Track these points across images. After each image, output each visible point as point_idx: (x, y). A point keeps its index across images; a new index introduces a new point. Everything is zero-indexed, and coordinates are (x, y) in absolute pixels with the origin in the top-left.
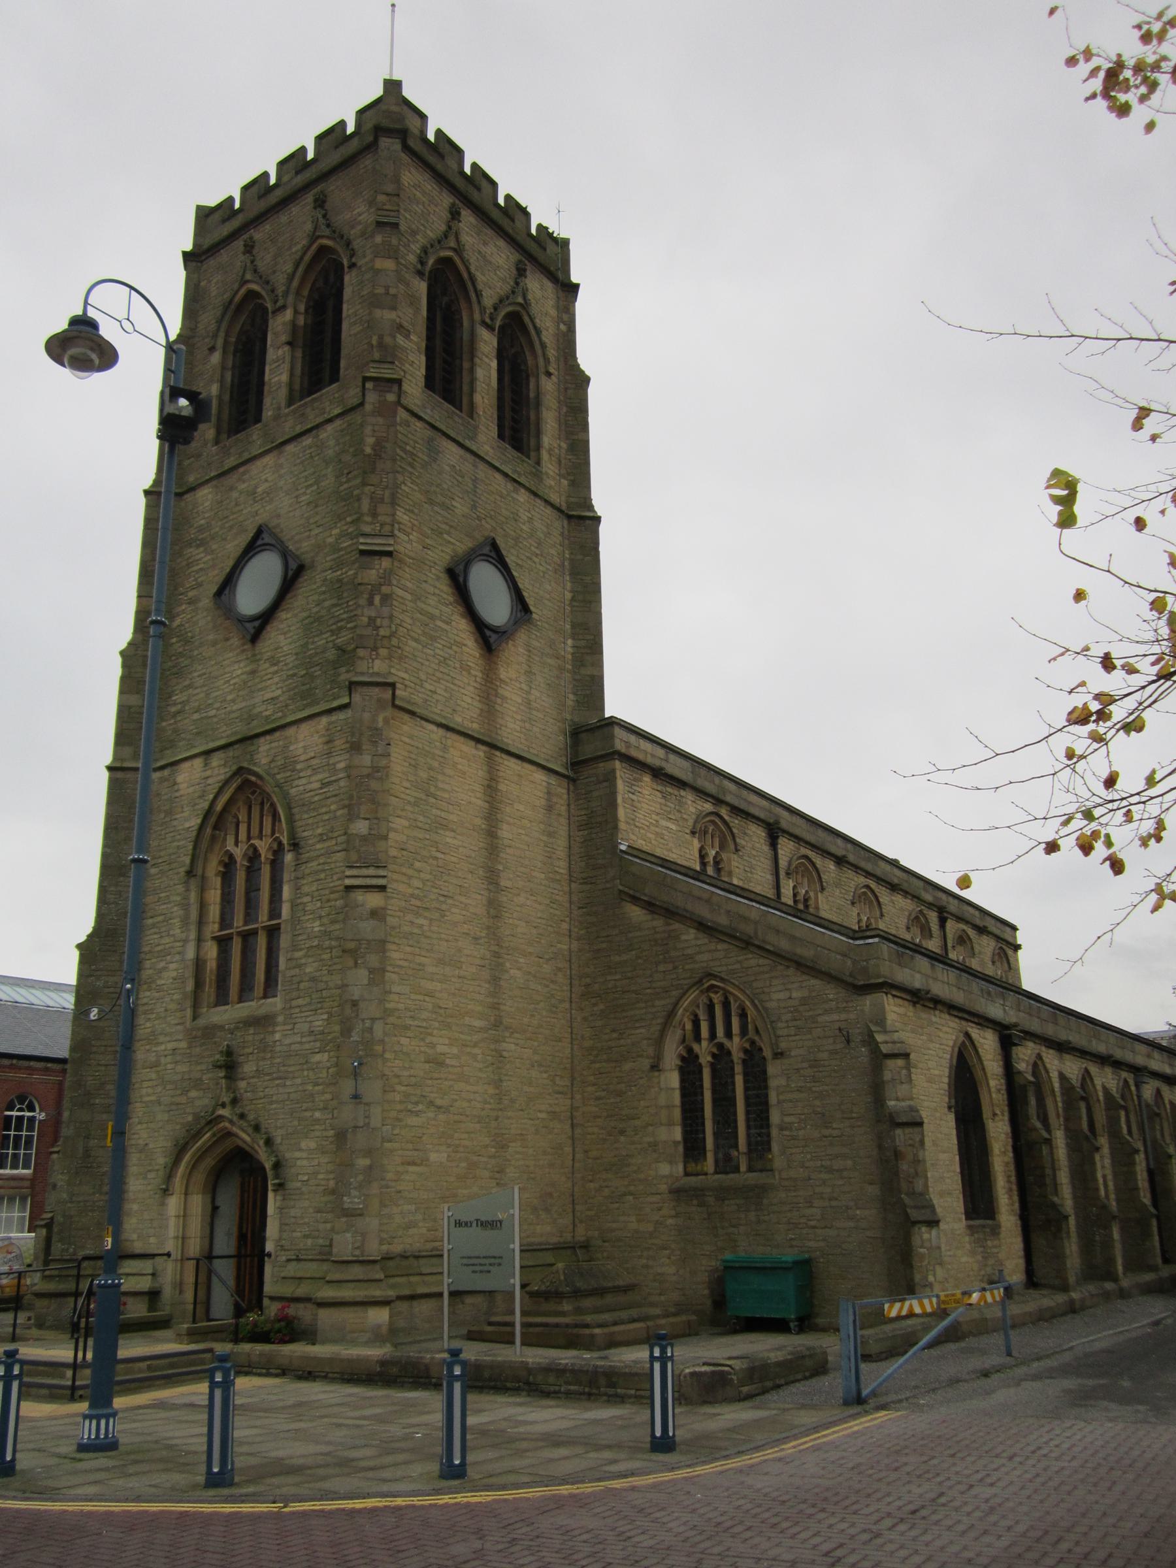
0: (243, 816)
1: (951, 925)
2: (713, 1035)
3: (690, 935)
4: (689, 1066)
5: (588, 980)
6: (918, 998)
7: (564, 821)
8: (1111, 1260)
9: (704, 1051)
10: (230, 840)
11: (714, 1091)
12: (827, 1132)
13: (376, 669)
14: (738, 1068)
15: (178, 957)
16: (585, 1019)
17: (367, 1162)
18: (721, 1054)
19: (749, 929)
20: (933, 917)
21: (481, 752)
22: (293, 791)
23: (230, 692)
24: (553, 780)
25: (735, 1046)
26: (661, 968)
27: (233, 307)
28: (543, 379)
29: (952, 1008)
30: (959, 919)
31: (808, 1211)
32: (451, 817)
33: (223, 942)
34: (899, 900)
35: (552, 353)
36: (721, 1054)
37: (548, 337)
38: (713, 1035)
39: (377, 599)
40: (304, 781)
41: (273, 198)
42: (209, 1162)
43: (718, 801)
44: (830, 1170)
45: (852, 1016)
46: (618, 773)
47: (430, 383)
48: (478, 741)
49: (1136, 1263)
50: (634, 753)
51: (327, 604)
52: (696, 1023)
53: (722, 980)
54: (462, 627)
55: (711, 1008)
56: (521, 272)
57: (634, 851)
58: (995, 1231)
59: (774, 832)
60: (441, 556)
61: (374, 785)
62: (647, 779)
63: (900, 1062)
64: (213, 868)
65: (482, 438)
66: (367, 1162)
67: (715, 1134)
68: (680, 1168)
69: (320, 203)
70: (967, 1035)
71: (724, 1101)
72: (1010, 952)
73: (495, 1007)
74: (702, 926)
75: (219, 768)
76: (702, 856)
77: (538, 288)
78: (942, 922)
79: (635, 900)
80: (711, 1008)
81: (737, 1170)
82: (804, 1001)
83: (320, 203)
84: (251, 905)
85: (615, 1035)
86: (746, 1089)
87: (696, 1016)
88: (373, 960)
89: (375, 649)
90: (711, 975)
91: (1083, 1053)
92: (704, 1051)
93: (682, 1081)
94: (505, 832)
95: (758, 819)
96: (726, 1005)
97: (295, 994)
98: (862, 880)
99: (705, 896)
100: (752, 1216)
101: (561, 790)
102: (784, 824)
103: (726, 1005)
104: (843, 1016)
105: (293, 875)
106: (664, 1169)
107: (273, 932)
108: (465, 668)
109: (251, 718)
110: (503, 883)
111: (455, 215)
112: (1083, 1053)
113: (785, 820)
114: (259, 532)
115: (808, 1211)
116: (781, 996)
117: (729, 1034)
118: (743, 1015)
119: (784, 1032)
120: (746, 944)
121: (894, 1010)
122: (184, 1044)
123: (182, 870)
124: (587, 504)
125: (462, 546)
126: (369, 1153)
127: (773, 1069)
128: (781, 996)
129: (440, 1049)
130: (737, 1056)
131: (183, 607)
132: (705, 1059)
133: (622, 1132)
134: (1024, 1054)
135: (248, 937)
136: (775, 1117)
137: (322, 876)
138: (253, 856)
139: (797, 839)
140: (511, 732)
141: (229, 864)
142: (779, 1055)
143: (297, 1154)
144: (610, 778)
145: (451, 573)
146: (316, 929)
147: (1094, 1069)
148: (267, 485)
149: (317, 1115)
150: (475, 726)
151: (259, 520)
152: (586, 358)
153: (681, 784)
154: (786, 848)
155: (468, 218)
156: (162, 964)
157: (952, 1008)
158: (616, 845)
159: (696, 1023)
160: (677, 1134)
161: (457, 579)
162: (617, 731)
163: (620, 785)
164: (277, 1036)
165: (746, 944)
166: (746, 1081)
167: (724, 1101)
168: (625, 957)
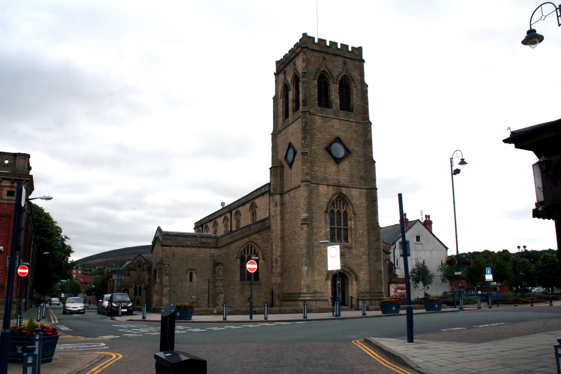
15: (324, 230)
23: (332, 173)
75: (331, 191)
105: (354, 220)
109: (339, 182)
123: (324, 210)
131: (315, 145)
137: (361, 222)
138: (339, 212)
143: (360, 274)
146: (361, 232)
149: (364, 267)
156: (320, 230)
164: (353, 251)
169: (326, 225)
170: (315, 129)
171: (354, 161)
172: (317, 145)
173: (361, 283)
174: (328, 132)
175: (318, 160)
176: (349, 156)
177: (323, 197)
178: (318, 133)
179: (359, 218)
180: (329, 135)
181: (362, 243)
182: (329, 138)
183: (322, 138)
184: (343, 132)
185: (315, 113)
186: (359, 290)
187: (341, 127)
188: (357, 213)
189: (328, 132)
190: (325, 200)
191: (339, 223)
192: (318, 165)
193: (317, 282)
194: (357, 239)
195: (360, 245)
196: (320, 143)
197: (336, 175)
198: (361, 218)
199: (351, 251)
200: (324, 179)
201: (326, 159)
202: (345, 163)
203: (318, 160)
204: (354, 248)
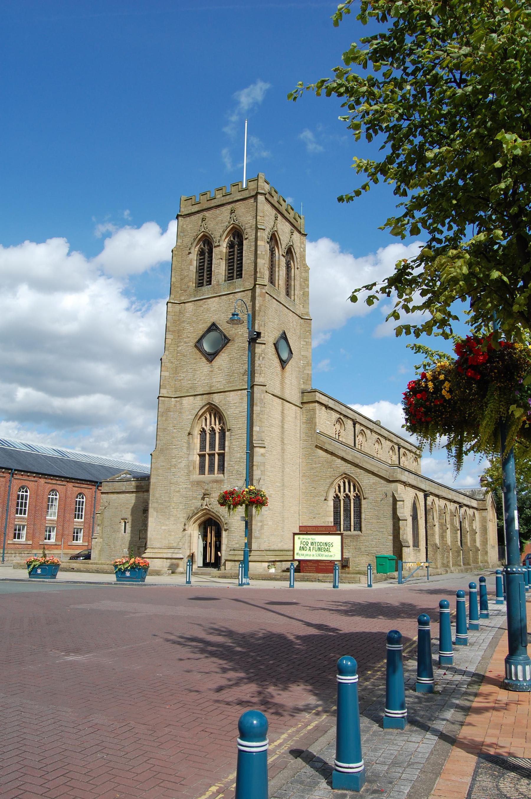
1: (402, 450)
2: (345, 491)
5: (304, 472)
6: (405, 484)
7: (299, 421)
8: (448, 562)
9: (342, 496)
11: (344, 508)
12: (378, 521)
13: (261, 381)
15: (186, 459)
16: (303, 483)
17: (261, 524)
18: (347, 496)
20: (396, 447)
21: (279, 401)
22: (228, 413)
23: (203, 377)
25: (352, 495)
26: (329, 470)
27: (198, 239)
29: (413, 487)
30: (404, 448)
31: (371, 543)
32: (274, 423)
33: (202, 456)
34: (388, 442)
38: (345, 491)
39: (261, 358)
40: (232, 410)
42: (199, 522)
44: (379, 532)
45: (388, 489)
46: (317, 407)
48: (280, 398)
49: (456, 564)
50: (321, 401)
51: (239, 354)
53: (349, 475)
54: (276, 362)
55: (344, 483)
56: (292, 233)
57: (321, 433)
59: (355, 423)
61: (261, 416)
62: (324, 408)
63: (401, 503)
64: (196, 432)
65: (281, 296)
66: (261, 524)
67: (344, 520)
69: (232, 212)
70: (416, 494)
71: (347, 511)
73: (283, 480)
74: (343, 459)
75: (199, 402)
78: (399, 449)
79: (321, 448)
80: (344, 483)
81: (350, 530)
82: (374, 483)
84: (212, 447)
85: (313, 489)
86: (354, 507)
87: (339, 485)
88: (262, 468)
89: (260, 374)
90: (345, 474)
91: (445, 498)
92: (342, 496)
93: (334, 504)
94: (286, 426)
95: (350, 418)
97: (231, 475)
99: (344, 449)
100: (355, 543)
104: (386, 489)
107: (222, 456)
110: (285, 442)
111: (276, 218)
112: (445, 498)
114: (214, 324)
115: (371, 543)
116: (367, 481)
117: (350, 491)
118: (354, 486)
119: (367, 492)
120: (357, 466)
121: (400, 487)
122: (190, 486)
126: (261, 521)
127: (363, 502)
128: (367, 481)
129: (271, 492)
130: (352, 498)
133: (314, 518)
134: (430, 499)
135: (212, 456)
136: (363, 516)
137: (240, 440)
138: (213, 430)
139: (361, 424)
141: (203, 431)
142: (364, 499)
144: (314, 410)
145: (274, 344)
147: (448, 503)
148: (215, 308)
150: (279, 393)
151: (212, 320)
157: (413, 487)
162: (317, 394)
163: (317, 412)
164: (225, 486)
165: (357, 466)
166: (354, 505)
167: (347, 511)
168: (317, 466)
169: (188, 453)
171: (235, 351)
172: (185, 343)
173: (234, 535)
174: (201, 320)
175: (185, 363)
176: (229, 345)
177: (188, 413)
178: (188, 326)
179: (236, 435)
180: (203, 323)
181: (239, 473)
182: (204, 327)
183: (192, 331)
184: (223, 313)
185: (187, 299)
186: (230, 546)
187: (220, 307)
188: (234, 428)
189: (201, 320)
190: (190, 417)
191: (212, 447)
192: (185, 370)
193: (173, 533)
194: (232, 468)
195: (235, 477)
196: (189, 339)
197: (208, 377)
198: (240, 435)
199: (222, 486)
200: (191, 388)
201: (196, 359)
202: (223, 358)
203: (185, 363)
204: (226, 481)
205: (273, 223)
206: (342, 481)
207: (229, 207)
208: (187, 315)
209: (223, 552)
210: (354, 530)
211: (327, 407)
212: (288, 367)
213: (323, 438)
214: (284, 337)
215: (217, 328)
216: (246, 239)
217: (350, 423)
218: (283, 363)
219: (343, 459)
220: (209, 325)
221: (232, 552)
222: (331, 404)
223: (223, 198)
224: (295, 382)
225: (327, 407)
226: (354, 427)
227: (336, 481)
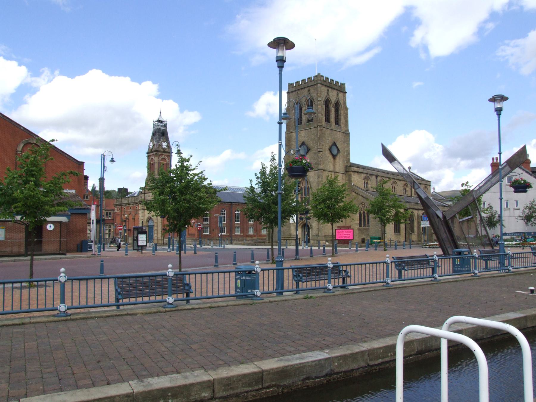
0: (303, 182)
3: (361, 197)
4: (360, 214)
9: (362, 212)
10: (301, 185)
14: (366, 214)
18: (364, 212)
19: (368, 197)
24: (343, 175)
28: (341, 111)
35: (343, 105)
36: (364, 212)
37: (342, 104)
41: (301, 87)
42: (301, 225)
43: (367, 174)
47: (326, 121)
52: (361, 208)
54: (330, 157)
56: (338, 94)
58: (400, 235)
59: (377, 177)
60: (327, 147)
62: (356, 173)
68: (359, 226)
69: (309, 91)
71: (364, 218)
72: (428, 187)
74: (362, 196)
76: (364, 182)
77: (341, 95)
83: (309, 91)
90: (363, 203)
92: (362, 212)
96: (365, 206)
98: (394, 180)
101: (344, 176)
102: (379, 175)
103: (365, 206)
106: (357, 226)
108: (331, 162)
111: (328, 91)
113: (379, 174)
124: (348, 130)
125: (330, 144)
132: (362, 213)
140: (337, 170)
145: (329, 149)
152: (348, 106)
153: (361, 173)
154: (379, 178)
155: (330, 90)
158: (351, 184)
159: (361, 208)
160: (358, 222)
161: (330, 150)
167: (364, 218)
170: (292, 141)
176: (310, 151)
205: (326, 94)
206: (362, 206)
207: (307, 89)
208: (293, 138)
209: (310, 237)
210: (367, 227)
211: (358, 172)
212: (338, 158)
213: (354, 187)
214: (335, 144)
215: (305, 144)
216: (314, 104)
217: (374, 177)
218: (334, 157)
219: (362, 196)
220: (302, 142)
221: (313, 237)
222: (361, 170)
223: (304, 85)
224: (341, 163)
225: (358, 172)
226: (377, 178)
227: (360, 205)
